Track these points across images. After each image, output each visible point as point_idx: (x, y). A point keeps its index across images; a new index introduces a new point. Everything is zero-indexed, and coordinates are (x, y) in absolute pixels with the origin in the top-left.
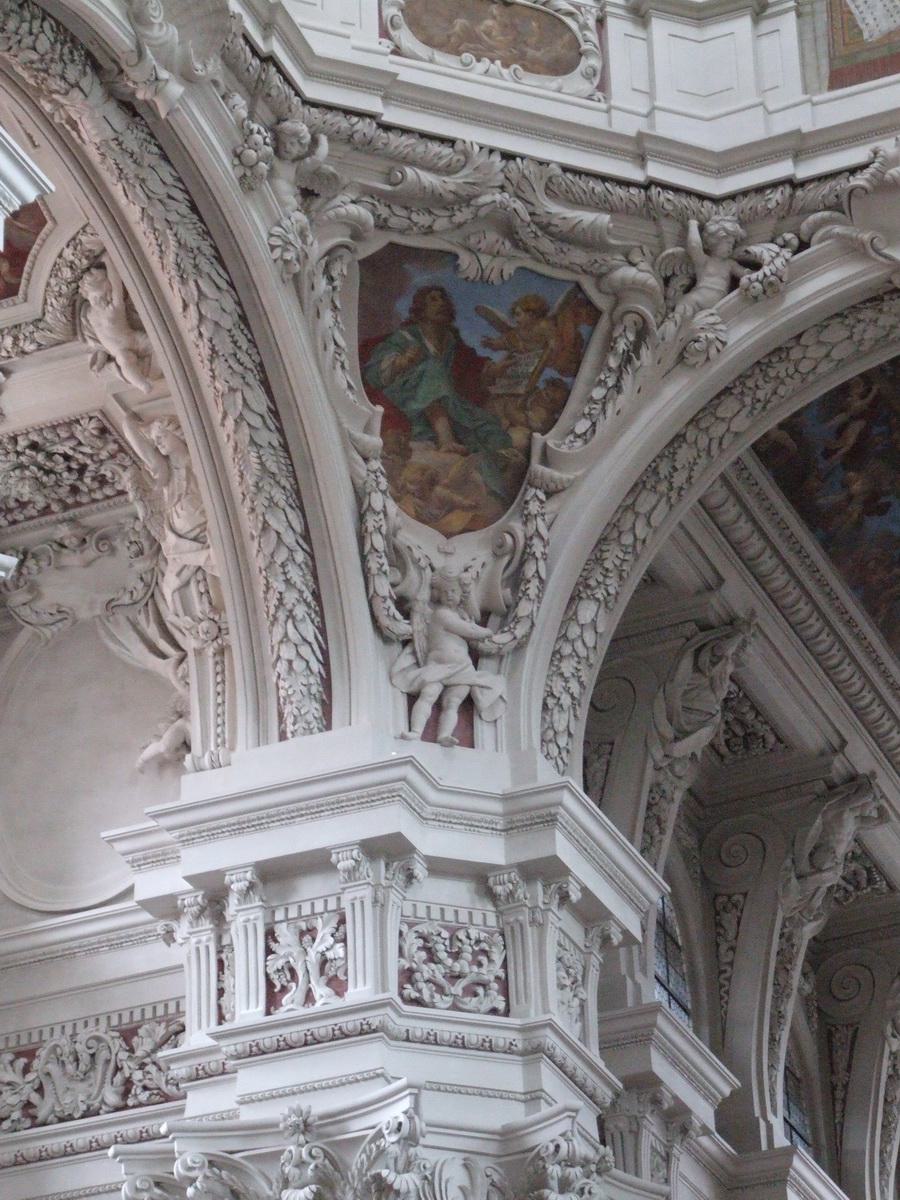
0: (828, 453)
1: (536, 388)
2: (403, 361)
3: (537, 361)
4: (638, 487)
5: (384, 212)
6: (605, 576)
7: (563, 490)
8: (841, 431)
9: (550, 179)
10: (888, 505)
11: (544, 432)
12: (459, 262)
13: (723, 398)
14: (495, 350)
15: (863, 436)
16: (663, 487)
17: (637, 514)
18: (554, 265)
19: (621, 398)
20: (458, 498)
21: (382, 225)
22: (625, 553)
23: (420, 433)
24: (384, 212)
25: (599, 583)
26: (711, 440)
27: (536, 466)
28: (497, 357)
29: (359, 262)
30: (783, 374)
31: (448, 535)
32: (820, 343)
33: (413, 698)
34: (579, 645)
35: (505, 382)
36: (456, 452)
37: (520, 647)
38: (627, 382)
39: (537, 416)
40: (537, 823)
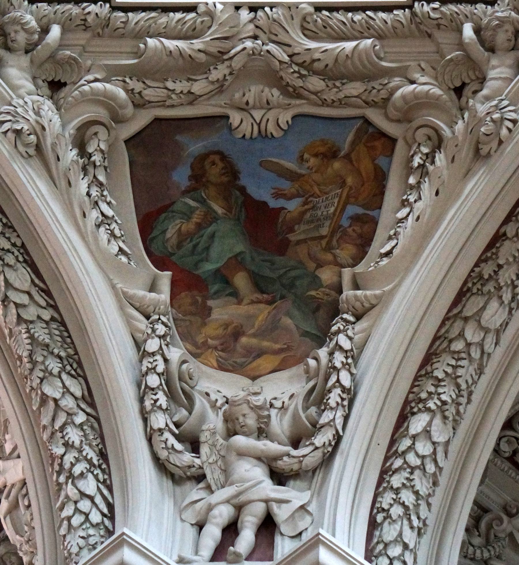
1: (341, 226)
2: (189, 226)
3: (336, 200)
4: (462, 295)
5: (136, 85)
6: (436, 386)
7: (373, 306)
9: (304, 19)
12: (231, 120)
14: (289, 198)
18: (332, 104)
19: (419, 205)
20: (266, 344)
21: (140, 103)
23: (215, 293)
24: (136, 85)
25: (430, 393)
28: (293, 206)
29: (126, 142)
31: (254, 378)
33: (200, 526)
35: (303, 227)
36: (260, 302)
37: (328, 460)
39: (345, 253)
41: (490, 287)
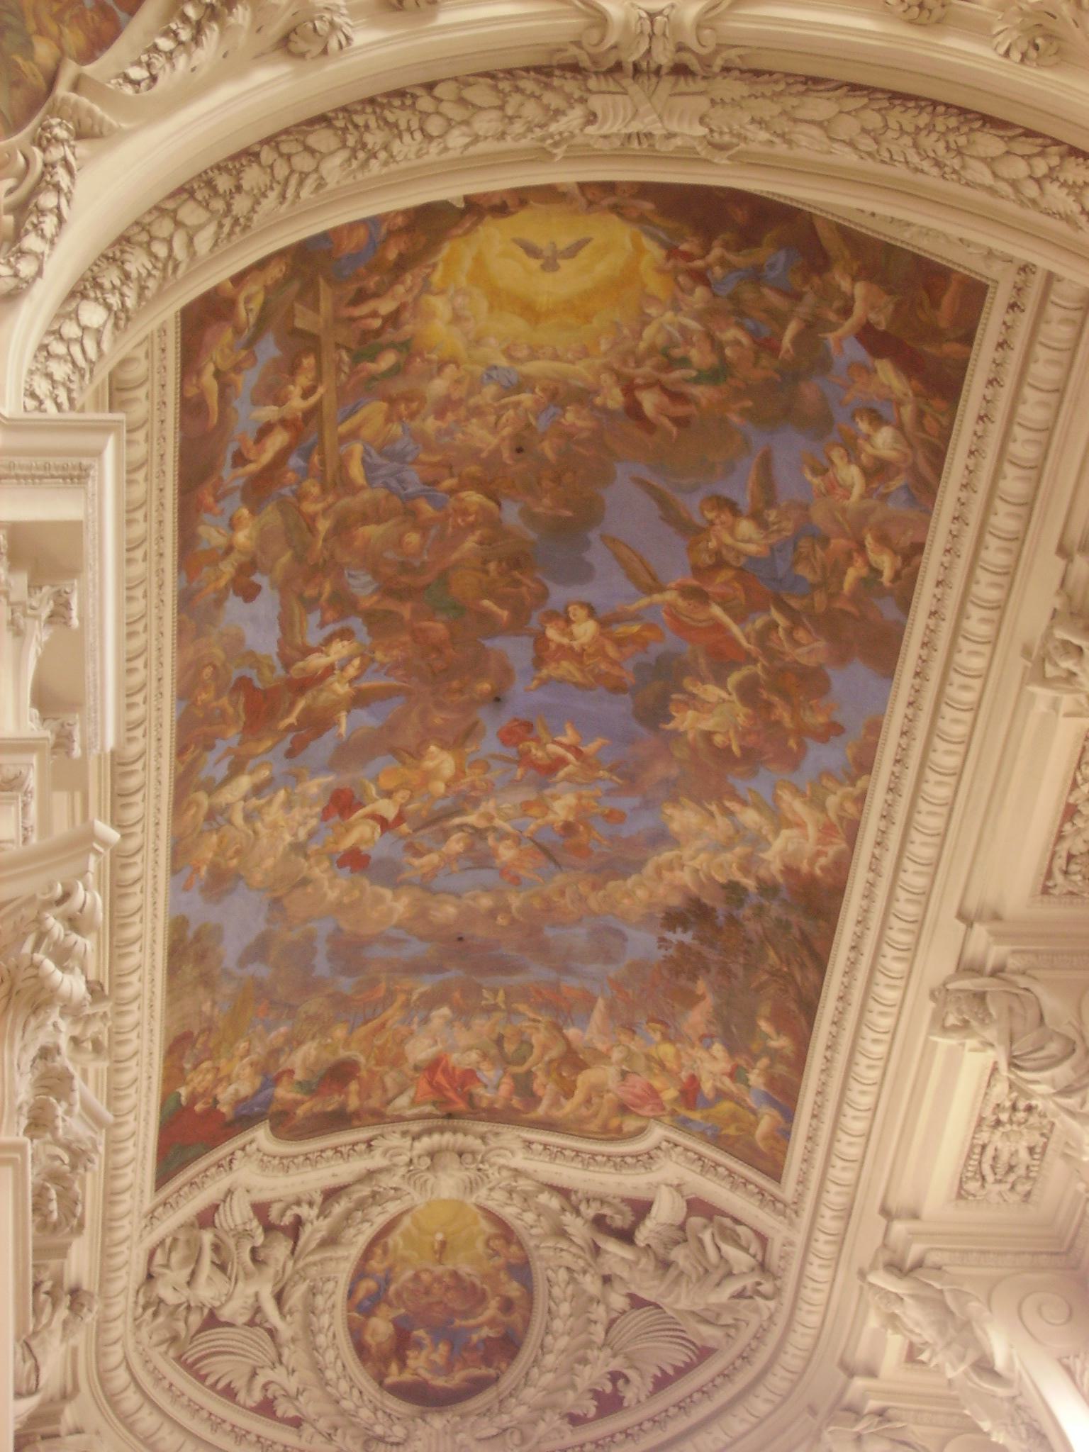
0: (240, 459)
4: (185, 192)
6: (123, 284)
7: (100, 136)
8: (265, 431)
10: (258, 588)
11: (88, 56)
13: (317, 127)
15: (282, 457)
16: (218, 205)
17: (178, 224)
22: (155, 267)
25: (114, 287)
26: (292, 171)
27: (62, 90)
30: (403, 126)
32: (462, 101)
34: (76, 350)
38: (212, 34)
40: (52, 477)
41: (218, 205)
